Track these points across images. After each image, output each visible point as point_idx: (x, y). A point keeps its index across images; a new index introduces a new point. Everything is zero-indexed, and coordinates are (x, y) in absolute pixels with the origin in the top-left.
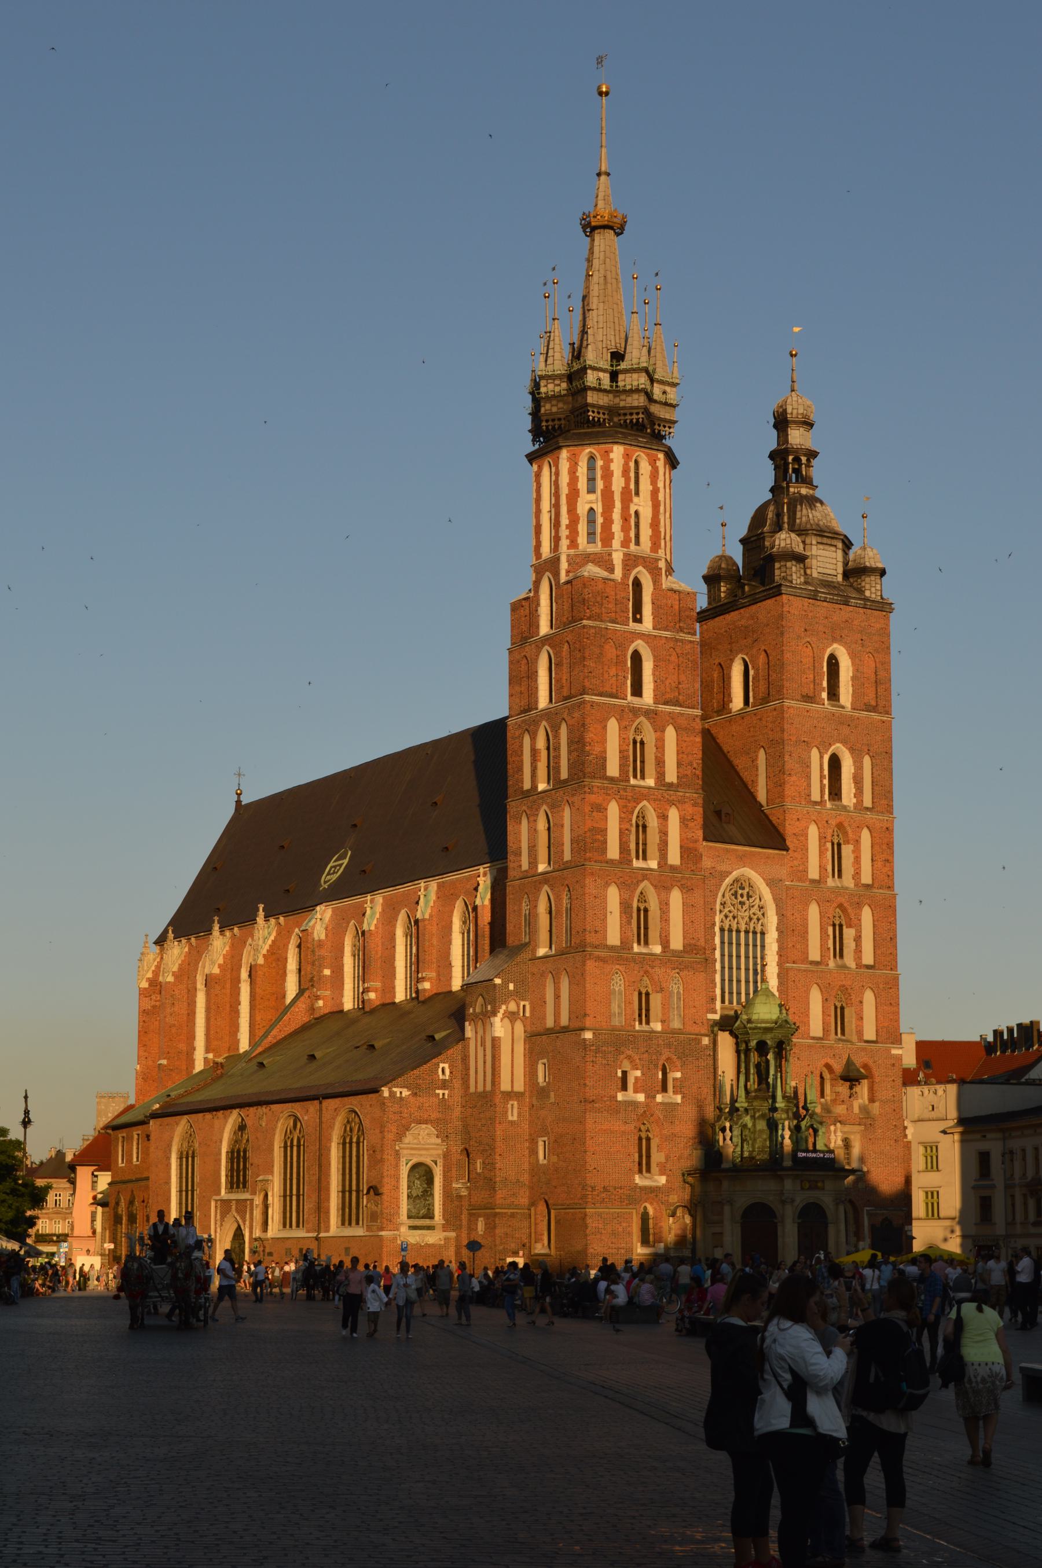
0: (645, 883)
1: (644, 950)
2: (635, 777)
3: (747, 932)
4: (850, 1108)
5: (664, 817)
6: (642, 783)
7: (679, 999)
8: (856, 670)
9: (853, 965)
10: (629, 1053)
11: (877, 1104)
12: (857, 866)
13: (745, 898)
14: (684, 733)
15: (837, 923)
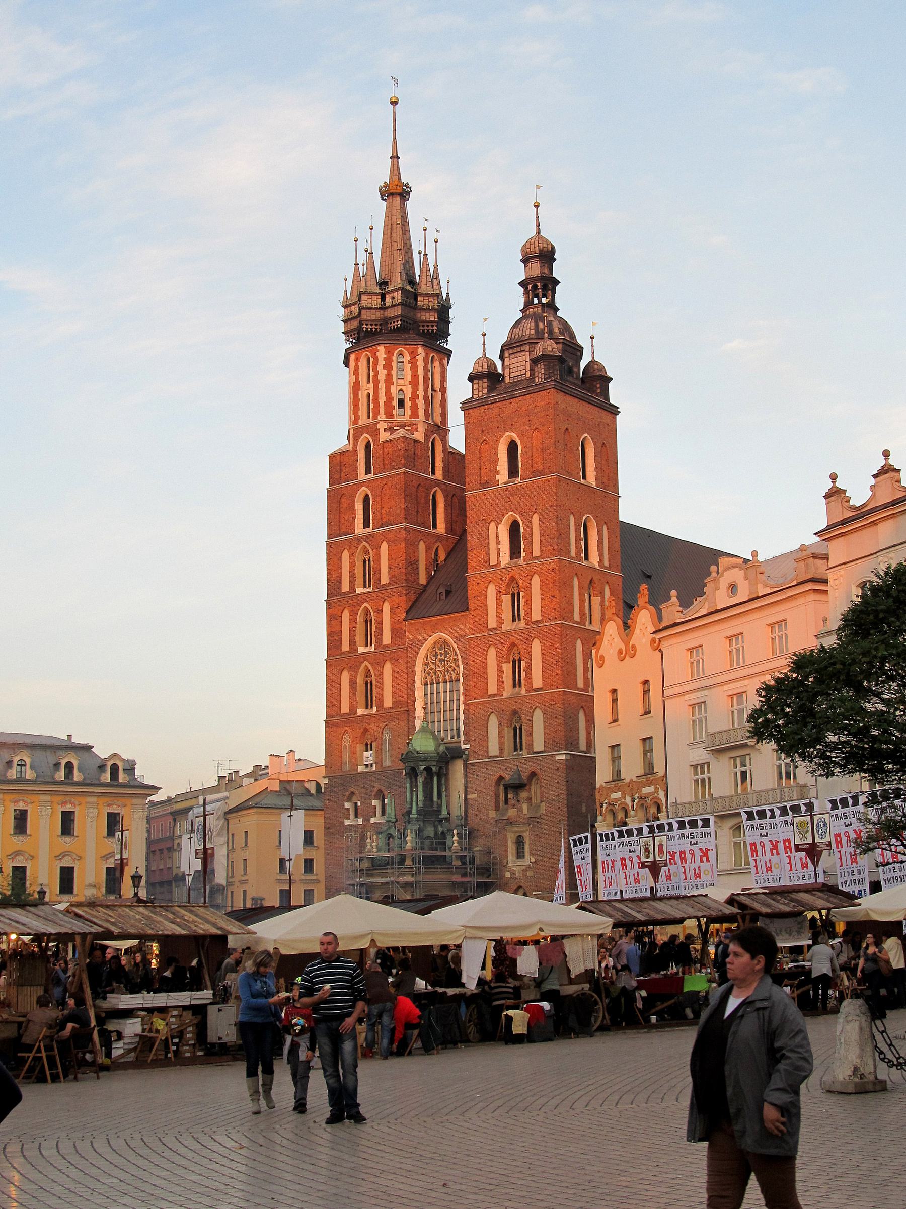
0: (366, 663)
1: (367, 712)
2: (365, 587)
3: (445, 682)
4: (520, 811)
5: (379, 611)
6: (368, 590)
7: (390, 744)
8: (524, 447)
9: (523, 691)
10: (352, 790)
11: (544, 804)
12: (527, 608)
13: (443, 657)
14: (393, 544)
15: (517, 658)
